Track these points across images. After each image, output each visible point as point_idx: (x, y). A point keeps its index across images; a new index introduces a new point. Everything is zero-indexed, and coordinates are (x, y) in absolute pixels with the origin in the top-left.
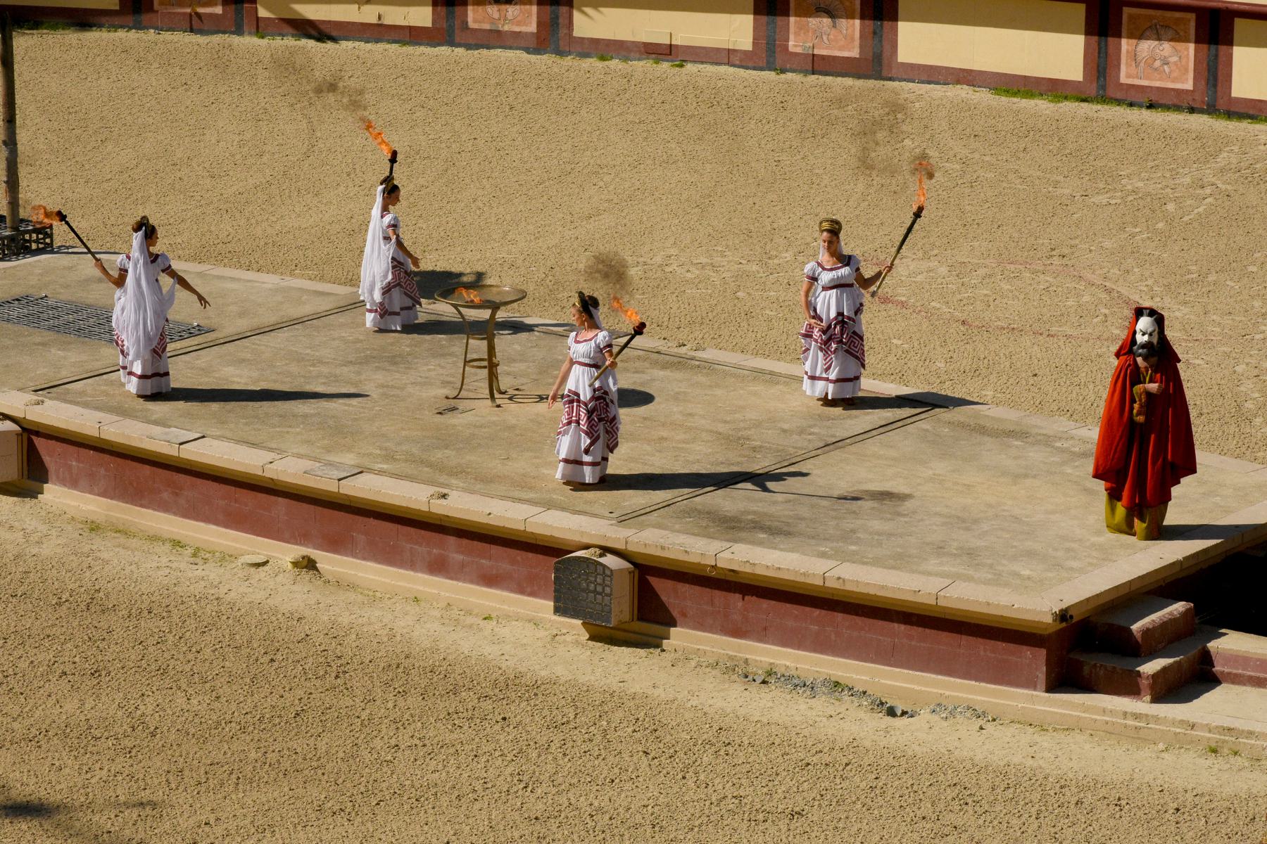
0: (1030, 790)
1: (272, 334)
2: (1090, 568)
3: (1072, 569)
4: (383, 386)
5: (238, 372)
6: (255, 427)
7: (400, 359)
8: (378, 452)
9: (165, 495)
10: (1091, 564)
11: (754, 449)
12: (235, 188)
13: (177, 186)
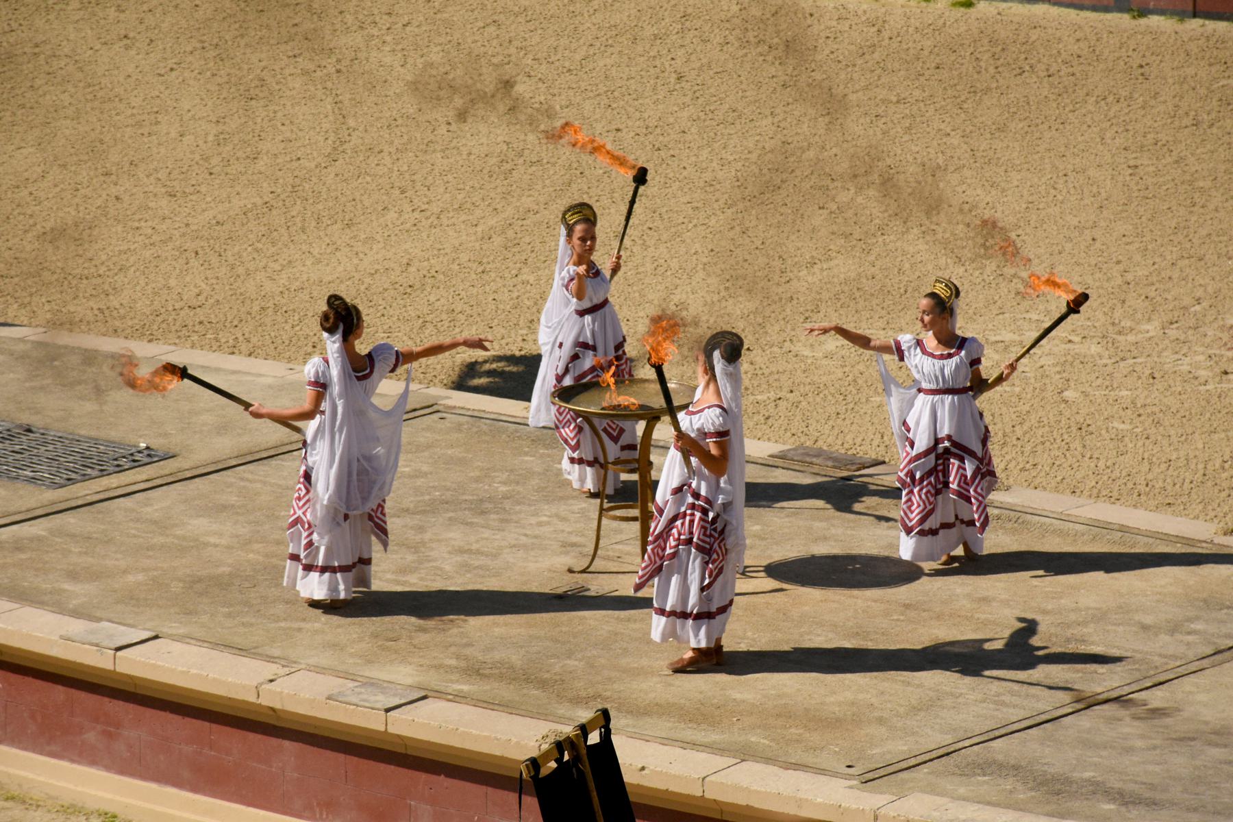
1: (273, 462)
4: (461, 551)
5: (215, 527)
6: (244, 620)
7: (490, 506)
9: (91, 736)
12: (209, 214)
13: (112, 212)
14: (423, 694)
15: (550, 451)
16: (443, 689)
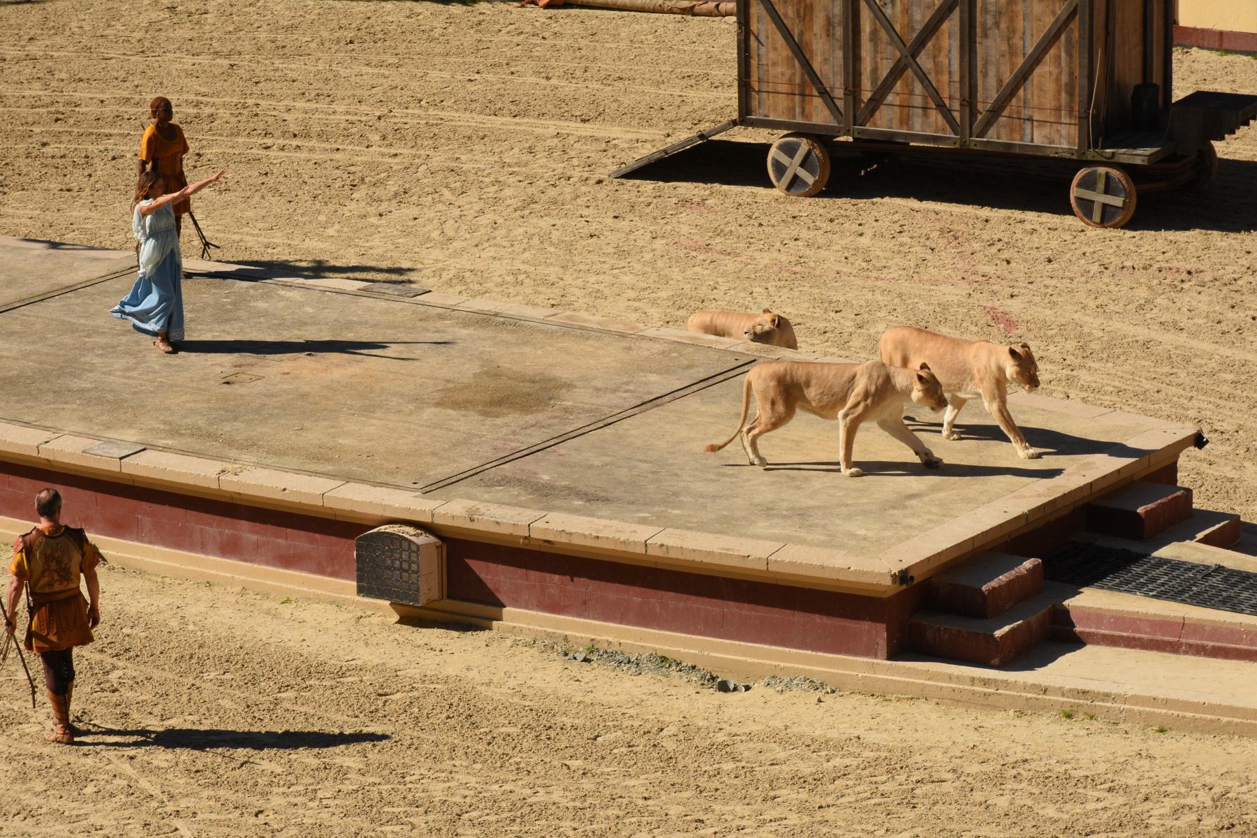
0: (874, 764)
1: (43, 304)
2: (930, 526)
3: (911, 527)
5: (7, 346)
8: (162, 427)
10: (930, 521)
11: (566, 410)
14: (142, 447)
15: (219, 291)
16: (155, 443)
